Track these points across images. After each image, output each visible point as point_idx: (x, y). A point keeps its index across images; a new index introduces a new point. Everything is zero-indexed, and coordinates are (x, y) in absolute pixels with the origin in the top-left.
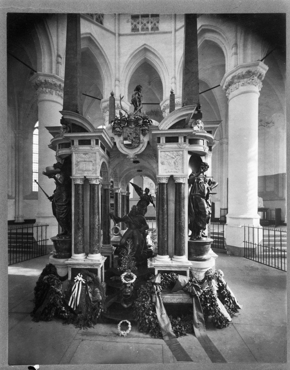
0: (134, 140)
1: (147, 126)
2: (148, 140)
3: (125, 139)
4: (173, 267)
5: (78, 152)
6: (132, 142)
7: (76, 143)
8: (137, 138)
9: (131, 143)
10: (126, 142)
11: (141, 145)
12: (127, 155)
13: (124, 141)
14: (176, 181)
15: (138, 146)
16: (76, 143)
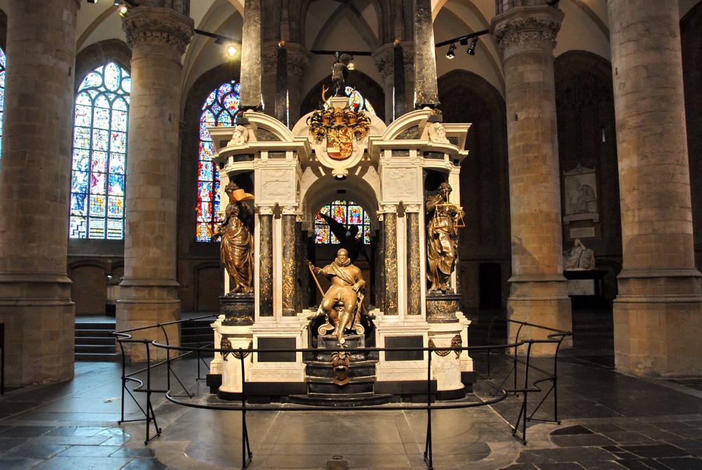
0: (343, 147)
1: (362, 126)
2: (366, 147)
3: (329, 145)
4: (405, 329)
5: (265, 168)
6: (341, 150)
7: (264, 155)
8: (347, 144)
9: (339, 151)
10: (331, 150)
11: (354, 154)
12: (332, 169)
13: (328, 148)
14: (408, 208)
15: (348, 157)
16: (264, 155)
